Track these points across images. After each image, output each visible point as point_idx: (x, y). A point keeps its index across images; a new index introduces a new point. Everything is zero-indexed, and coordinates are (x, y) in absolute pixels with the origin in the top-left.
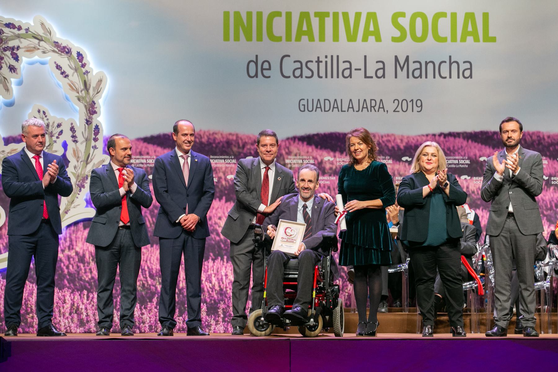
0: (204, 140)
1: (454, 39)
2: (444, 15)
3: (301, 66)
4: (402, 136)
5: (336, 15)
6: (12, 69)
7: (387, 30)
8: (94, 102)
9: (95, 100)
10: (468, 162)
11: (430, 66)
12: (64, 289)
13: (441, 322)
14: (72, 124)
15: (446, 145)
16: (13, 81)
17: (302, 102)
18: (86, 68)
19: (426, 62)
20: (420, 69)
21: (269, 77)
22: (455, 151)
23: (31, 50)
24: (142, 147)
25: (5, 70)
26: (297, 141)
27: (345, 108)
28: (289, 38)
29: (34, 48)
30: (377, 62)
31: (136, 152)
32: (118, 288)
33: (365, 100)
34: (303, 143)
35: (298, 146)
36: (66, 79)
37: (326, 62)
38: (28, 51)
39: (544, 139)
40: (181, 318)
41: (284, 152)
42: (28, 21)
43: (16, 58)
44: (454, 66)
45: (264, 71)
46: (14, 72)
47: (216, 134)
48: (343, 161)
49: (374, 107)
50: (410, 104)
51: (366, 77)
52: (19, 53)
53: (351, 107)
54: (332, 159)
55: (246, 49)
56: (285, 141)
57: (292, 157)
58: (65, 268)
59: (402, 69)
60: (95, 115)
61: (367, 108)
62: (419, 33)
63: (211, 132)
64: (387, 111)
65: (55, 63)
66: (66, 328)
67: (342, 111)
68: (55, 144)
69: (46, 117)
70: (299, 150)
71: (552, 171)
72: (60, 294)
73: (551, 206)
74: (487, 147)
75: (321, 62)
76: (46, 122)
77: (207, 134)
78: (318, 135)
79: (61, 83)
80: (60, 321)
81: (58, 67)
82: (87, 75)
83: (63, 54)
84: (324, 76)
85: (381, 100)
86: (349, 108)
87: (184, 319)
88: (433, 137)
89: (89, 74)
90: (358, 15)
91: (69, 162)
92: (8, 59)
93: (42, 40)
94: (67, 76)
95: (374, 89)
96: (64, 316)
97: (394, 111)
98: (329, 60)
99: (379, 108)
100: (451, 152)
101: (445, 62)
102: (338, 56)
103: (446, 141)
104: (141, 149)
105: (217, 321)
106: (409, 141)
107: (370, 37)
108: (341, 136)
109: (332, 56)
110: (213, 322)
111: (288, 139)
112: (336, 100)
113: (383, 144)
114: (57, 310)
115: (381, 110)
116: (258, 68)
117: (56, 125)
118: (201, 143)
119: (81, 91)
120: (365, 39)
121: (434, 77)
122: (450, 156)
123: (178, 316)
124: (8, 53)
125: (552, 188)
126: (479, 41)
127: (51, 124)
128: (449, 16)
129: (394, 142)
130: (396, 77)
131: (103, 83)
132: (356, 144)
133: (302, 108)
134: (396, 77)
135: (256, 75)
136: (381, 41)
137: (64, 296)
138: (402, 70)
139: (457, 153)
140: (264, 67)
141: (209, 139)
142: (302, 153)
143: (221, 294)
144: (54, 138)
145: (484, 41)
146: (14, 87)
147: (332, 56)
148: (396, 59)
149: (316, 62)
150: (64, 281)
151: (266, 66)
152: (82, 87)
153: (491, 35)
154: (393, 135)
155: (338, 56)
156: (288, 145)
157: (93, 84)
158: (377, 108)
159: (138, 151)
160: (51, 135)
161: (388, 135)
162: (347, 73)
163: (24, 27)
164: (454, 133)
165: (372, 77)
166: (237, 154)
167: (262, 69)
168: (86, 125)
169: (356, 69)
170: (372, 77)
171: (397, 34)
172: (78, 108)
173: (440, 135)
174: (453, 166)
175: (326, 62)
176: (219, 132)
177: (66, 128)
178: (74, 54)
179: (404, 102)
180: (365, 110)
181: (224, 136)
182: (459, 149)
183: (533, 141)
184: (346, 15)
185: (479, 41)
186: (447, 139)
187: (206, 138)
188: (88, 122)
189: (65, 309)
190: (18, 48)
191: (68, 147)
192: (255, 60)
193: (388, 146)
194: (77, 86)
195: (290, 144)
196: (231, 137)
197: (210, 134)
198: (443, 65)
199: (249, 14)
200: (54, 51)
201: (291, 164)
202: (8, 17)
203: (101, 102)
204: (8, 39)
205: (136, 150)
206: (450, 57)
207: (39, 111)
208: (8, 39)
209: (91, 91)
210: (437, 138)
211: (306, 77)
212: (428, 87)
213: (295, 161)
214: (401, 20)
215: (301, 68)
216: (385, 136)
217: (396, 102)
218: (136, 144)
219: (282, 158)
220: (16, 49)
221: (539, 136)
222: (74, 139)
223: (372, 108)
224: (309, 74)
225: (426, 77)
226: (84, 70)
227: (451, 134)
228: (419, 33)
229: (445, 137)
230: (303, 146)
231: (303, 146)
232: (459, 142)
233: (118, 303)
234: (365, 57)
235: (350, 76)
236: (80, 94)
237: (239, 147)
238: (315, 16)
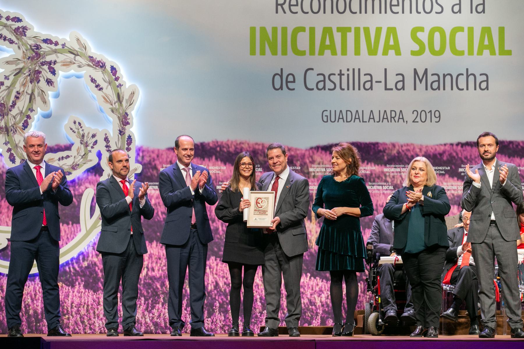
0: (232, 149)
1: (471, 53)
2: (461, 29)
3: (324, 78)
4: (421, 145)
5: (357, 30)
6: (49, 82)
7: (407, 44)
8: (126, 114)
9: (128, 111)
11: (448, 78)
12: (98, 291)
13: (460, 324)
14: (106, 134)
15: (463, 154)
16: (50, 94)
17: (325, 113)
18: (120, 81)
19: (444, 74)
20: (439, 81)
21: (294, 89)
22: (472, 159)
23: (67, 64)
24: (172, 156)
25: (43, 83)
26: (320, 150)
27: (366, 119)
28: (312, 53)
29: (70, 62)
30: (397, 75)
31: (166, 161)
32: (150, 291)
33: (385, 111)
34: (326, 152)
35: (322, 155)
36: (100, 92)
37: (348, 75)
38: (64, 65)
40: (209, 319)
41: (308, 161)
42: (64, 36)
43: (53, 72)
44: (471, 78)
45: (289, 84)
46: (51, 85)
47: (243, 143)
48: (364, 170)
49: (394, 118)
50: (429, 115)
51: (386, 89)
52: (56, 67)
53: (372, 117)
55: (272, 63)
56: (309, 151)
57: (316, 166)
58: (99, 271)
59: (421, 81)
60: (128, 126)
61: (387, 118)
62: (437, 47)
63: (238, 142)
64: (407, 122)
65: (90, 76)
66: (100, 329)
67: (363, 122)
68: (90, 154)
69: (81, 127)
70: (322, 159)
72: (94, 296)
74: (503, 156)
75: (344, 75)
76: (81, 133)
77: (235, 144)
79: (95, 96)
80: (94, 322)
81: (93, 80)
82: (120, 88)
83: (97, 68)
84: (346, 88)
85: (401, 111)
86: (370, 118)
87: (212, 320)
88: (451, 146)
89: (122, 87)
90: (379, 30)
91: (104, 170)
92: (46, 73)
93: (78, 55)
94: (101, 89)
95: (394, 101)
96: (98, 317)
97: (413, 122)
99: (399, 118)
100: (468, 160)
101: (462, 74)
102: (359, 70)
103: (464, 150)
104: (172, 158)
106: (427, 150)
108: (363, 146)
109: (354, 70)
111: (311, 148)
112: (357, 111)
113: (403, 153)
114: (92, 312)
115: (401, 120)
116: (283, 81)
117: (90, 135)
118: (229, 152)
119: (115, 103)
120: (385, 53)
121: (452, 89)
123: (207, 318)
124: (46, 67)
126: (495, 55)
127: (86, 135)
128: (466, 30)
129: (413, 151)
130: (415, 89)
131: (135, 95)
132: (275, 158)
133: (325, 120)
134: (415, 89)
135: (281, 88)
137: (98, 298)
138: (421, 83)
139: (473, 162)
140: (289, 80)
141: (236, 148)
142: (325, 162)
144: (89, 148)
145: (500, 54)
146: (51, 100)
147: (354, 70)
148: (415, 71)
149: (338, 75)
150: (98, 284)
151: (290, 78)
152: (116, 99)
153: (507, 48)
154: (412, 144)
155: (359, 70)
156: (311, 154)
157: (126, 96)
158: (396, 119)
159: (169, 160)
160: (86, 145)
161: (408, 145)
162: (368, 85)
163: (60, 43)
164: (470, 142)
165: (392, 89)
166: (263, 162)
167: (287, 82)
168: (120, 136)
169: (376, 82)
170: (392, 89)
171: (416, 48)
172: (111, 119)
173: (458, 144)
175: (348, 75)
176: (246, 142)
177: (100, 139)
178: (108, 68)
179: (423, 113)
180: (385, 120)
181: (251, 146)
182: (476, 158)
184: (367, 30)
185: (495, 55)
186: (464, 148)
187: (233, 147)
188: (121, 133)
189: (99, 310)
190: (55, 62)
191: (103, 157)
192: (280, 73)
193: (407, 155)
194: (111, 99)
195: (313, 153)
196: (257, 147)
197: (237, 144)
199: (275, 29)
200: (89, 65)
201: (314, 172)
202: (45, 33)
203: (134, 114)
204: (46, 54)
205: (166, 159)
206: (467, 70)
207: (75, 123)
208: (46, 54)
209: (124, 103)
210: (455, 147)
211: (329, 89)
212: (444, 99)
213: (318, 170)
214: (419, 35)
215: (324, 81)
216: (405, 145)
217: (415, 113)
218: (167, 153)
219: (306, 167)
220: (53, 64)
222: (107, 149)
223: (392, 119)
224: (332, 86)
225: (444, 89)
226: (117, 83)
227: (468, 144)
228: (437, 47)
230: (326, 155)
231: (326, 155)
233: (150, 305)
234: (386, 70)
235: (371, 88)
236: (114, 106)
238: (338, 31)
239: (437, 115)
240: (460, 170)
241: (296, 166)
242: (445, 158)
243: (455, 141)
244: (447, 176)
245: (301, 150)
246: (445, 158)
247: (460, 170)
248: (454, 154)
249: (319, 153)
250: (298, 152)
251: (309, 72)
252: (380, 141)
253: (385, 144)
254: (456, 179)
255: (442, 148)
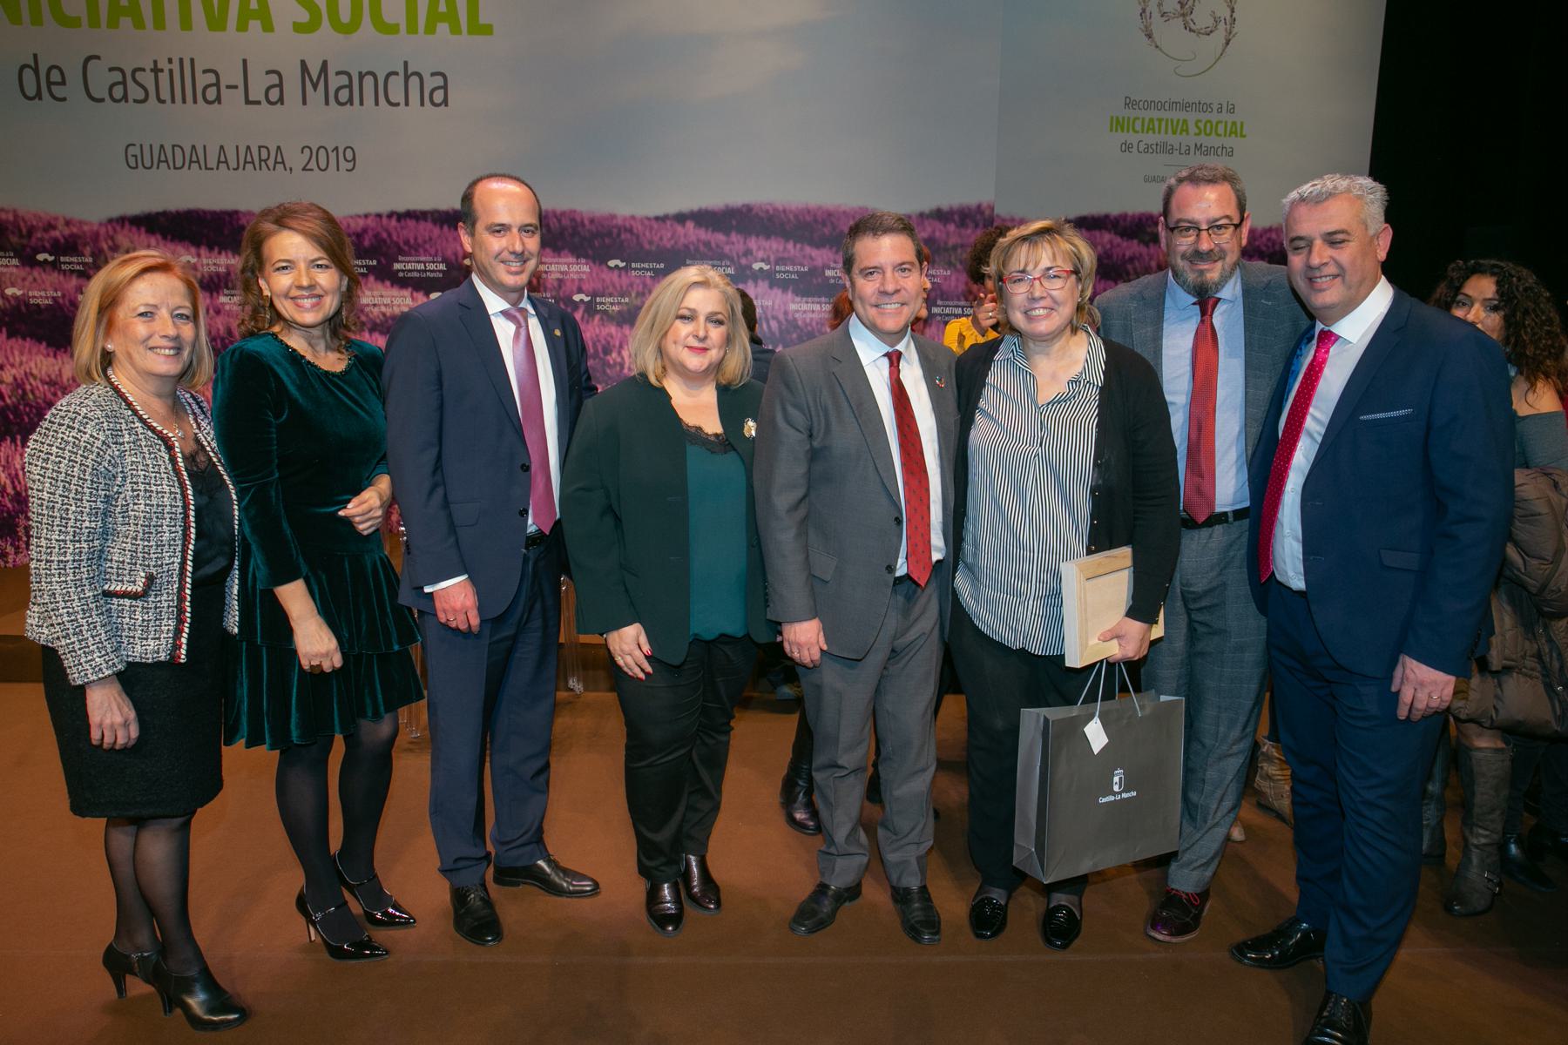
1: (412, 28)
3: (124, 78)
10: (442, 267)
11: (369, 80)
17: (131, 150)
20: (350, 86)
21: (64, 99)
27: (212, 162)
30: (268, 73)
37: (171, 71)
39: (583, 225)
41: (105, 247)
44: (414, 81)
50: (333, 156)
51: (248, 102)
54: (194, 260)
59: (315, 86)
62: (345, 16)
71: (599, 286)
73: (596, 351)
78: (164, 214)
98: (176, 67)
102: (192, 60)
105: (17, 548)
107: (252, 23)
109: (181, 60)
110: (10, 549)
111: (110, 221)
120: (242, 26)
121: (377, 103)
122: (410, 255)
125: (597, 317)
130: (304, 103)
133: (132, 162)
134: (304, 103)
136: (272, 30)
143: (19, 502)
145: (469, 33)
147: (181, 60)
151: (55, 76)
153: (483, 20)
155: (192, 60)
158: (271, 163)
165: (258, 103)
170: (258, 103)
171: (304, 16)
173: (391, 215)
174: (416, 275)
175: (171, 71)
180: (249, 166)
183: (563, 229)
198: (392, 78)
206: (406, 63)
210: (385, 220)
215: (124, 83)
217: (307, 151)
221: (573, 220)
224: (141, 95)
225: (361, 103)
227: (410, 215)
228: (345, 16)
229: (399, 220)
232: (425, 228)
234: (245, 61)
235: (218, 99)
237: (21, 236)
239: (349, 157)
240: (397, 266)
241: (83, 255)
242: (367, 243)
243: (384, 207)
244: (372, 278)
245: (90, 224)
246: (367, 243)
247: (397, 266)
248: (385, 235)
249: (126, 231)
250: (86, 228)
251: (91, 64)
252: (242, 207)
253: (250, 214)
254: (388, 283)
255: (361, 222)
